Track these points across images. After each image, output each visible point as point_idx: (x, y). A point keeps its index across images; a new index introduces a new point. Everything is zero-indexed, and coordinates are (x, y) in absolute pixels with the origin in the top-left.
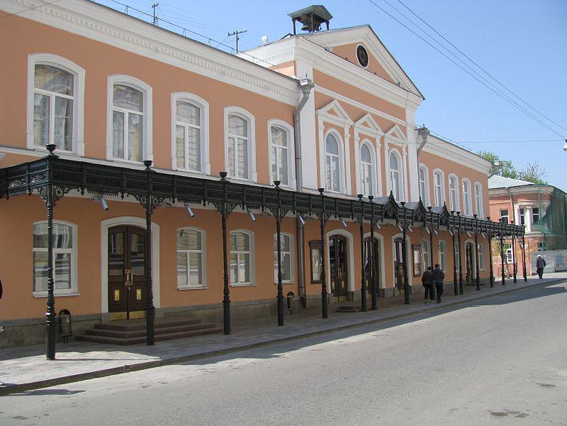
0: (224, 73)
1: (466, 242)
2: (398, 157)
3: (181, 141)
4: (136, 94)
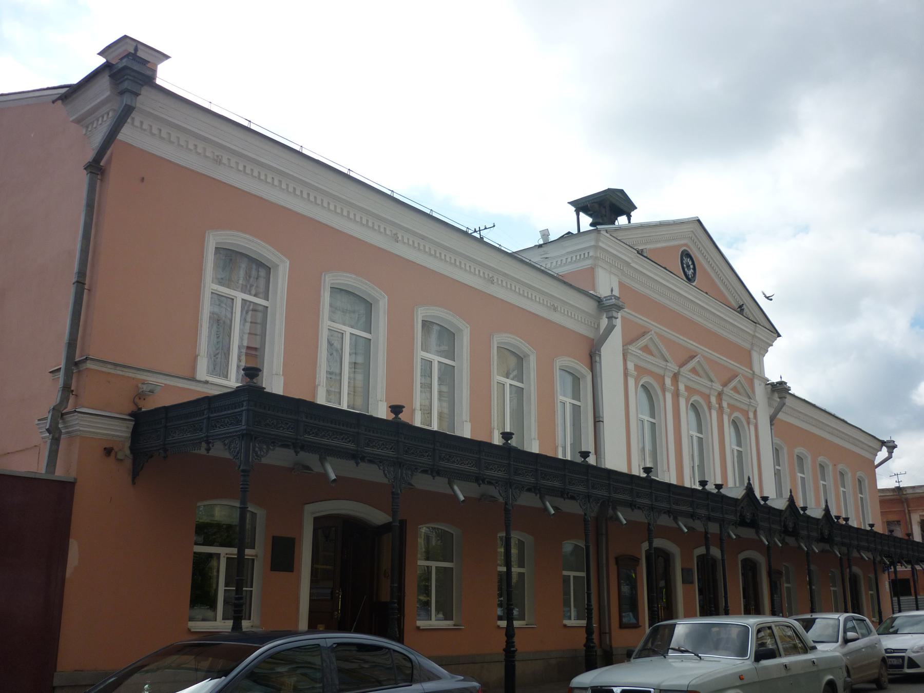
0: (218, 161)
1: (742, 556)
2: (657, 395)
3: (335, 353)
4: (260, 269)
